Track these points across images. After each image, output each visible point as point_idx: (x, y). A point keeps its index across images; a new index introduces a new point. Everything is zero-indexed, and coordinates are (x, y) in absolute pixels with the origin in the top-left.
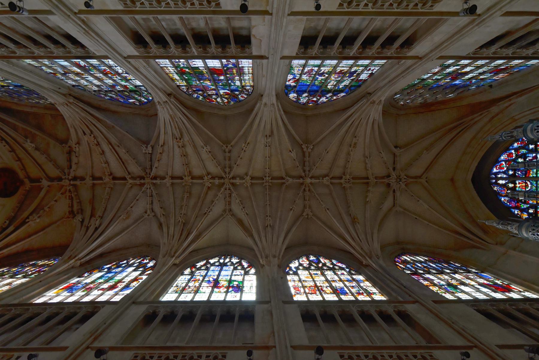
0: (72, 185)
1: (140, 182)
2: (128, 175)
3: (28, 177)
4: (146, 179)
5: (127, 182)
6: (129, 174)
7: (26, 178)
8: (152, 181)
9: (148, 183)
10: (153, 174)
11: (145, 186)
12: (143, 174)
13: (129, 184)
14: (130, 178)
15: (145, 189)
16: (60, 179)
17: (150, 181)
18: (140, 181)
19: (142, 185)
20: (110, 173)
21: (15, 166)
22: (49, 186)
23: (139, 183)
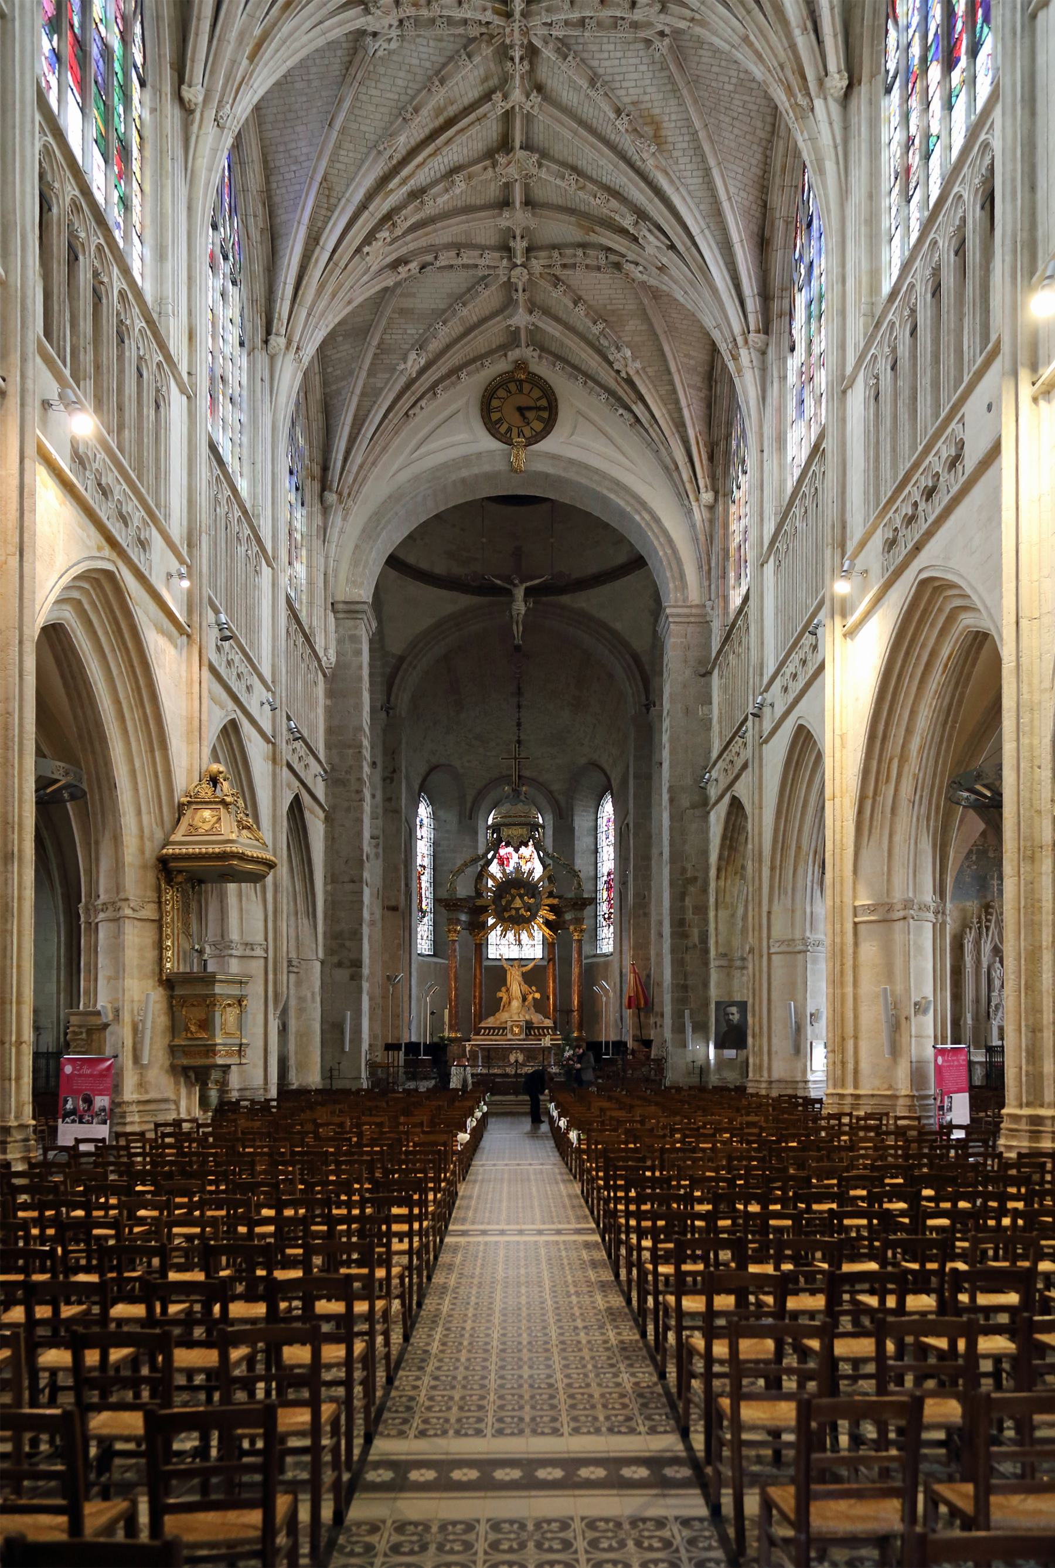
0: (528, 259)
1: (522, 59)
2: (494, 105)
3: (503, 349)
4: (508, 41)
5: (521, 108)
6: (487, 97)
7: (505, 355)
8: (517, 15)
9: (525, 32)
10: (489, 13)
11: (537, 43)
12: (488, 51)
13: (530, 104)
14: (505, 97)
15: (551, 45)
16: (509, 286)
17: (517, 25)
18: (517, 60)
19: (532, 52)
20: (488, 162)
21: (473, 383)
22: (531, 312)
23: (525, 63)
